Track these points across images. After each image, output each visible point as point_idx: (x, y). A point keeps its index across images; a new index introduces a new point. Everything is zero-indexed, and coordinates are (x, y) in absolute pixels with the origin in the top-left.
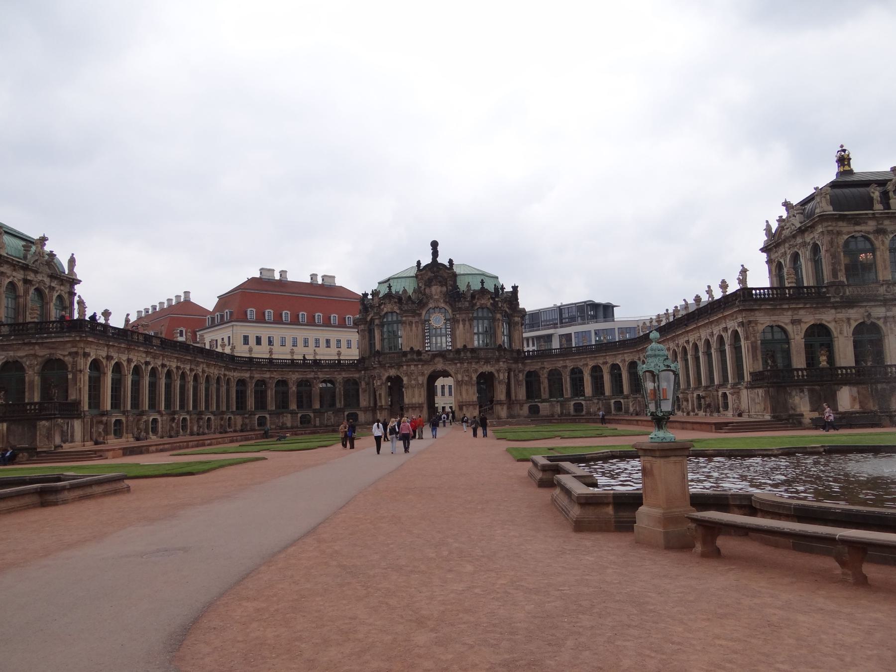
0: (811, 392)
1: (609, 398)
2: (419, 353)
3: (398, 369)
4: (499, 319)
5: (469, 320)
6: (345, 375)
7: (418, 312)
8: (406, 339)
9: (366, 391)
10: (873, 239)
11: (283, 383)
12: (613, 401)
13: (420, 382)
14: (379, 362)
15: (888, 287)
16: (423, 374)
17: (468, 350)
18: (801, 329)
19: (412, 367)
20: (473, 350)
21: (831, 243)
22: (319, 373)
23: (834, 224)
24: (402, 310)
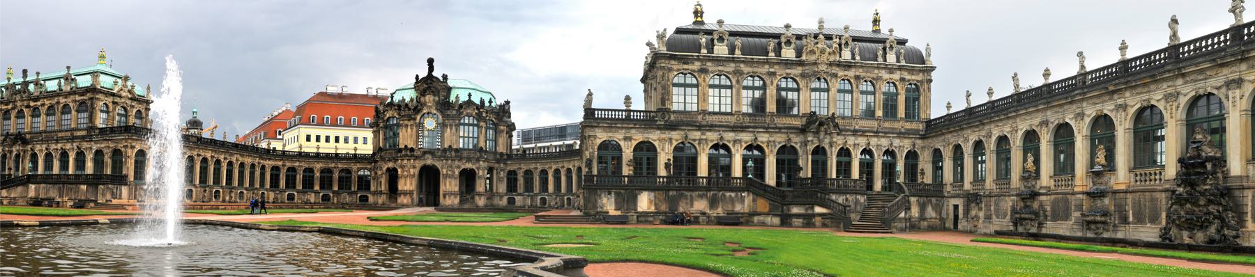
2: (412, 150)
4: (482, 127)
5: (456, 125)
6: (359, 166)
7: (413, 116)
8: (406, 138)
10: (697, 76)
12: (566, 197)
13: (412, 173)
14: (380, 156)
15: (704, 115)
16: (414, 167)
17: (453, 149)
18: (632, 145)
19: (406, 161)
20: (457, 150)
23: (667, 62)
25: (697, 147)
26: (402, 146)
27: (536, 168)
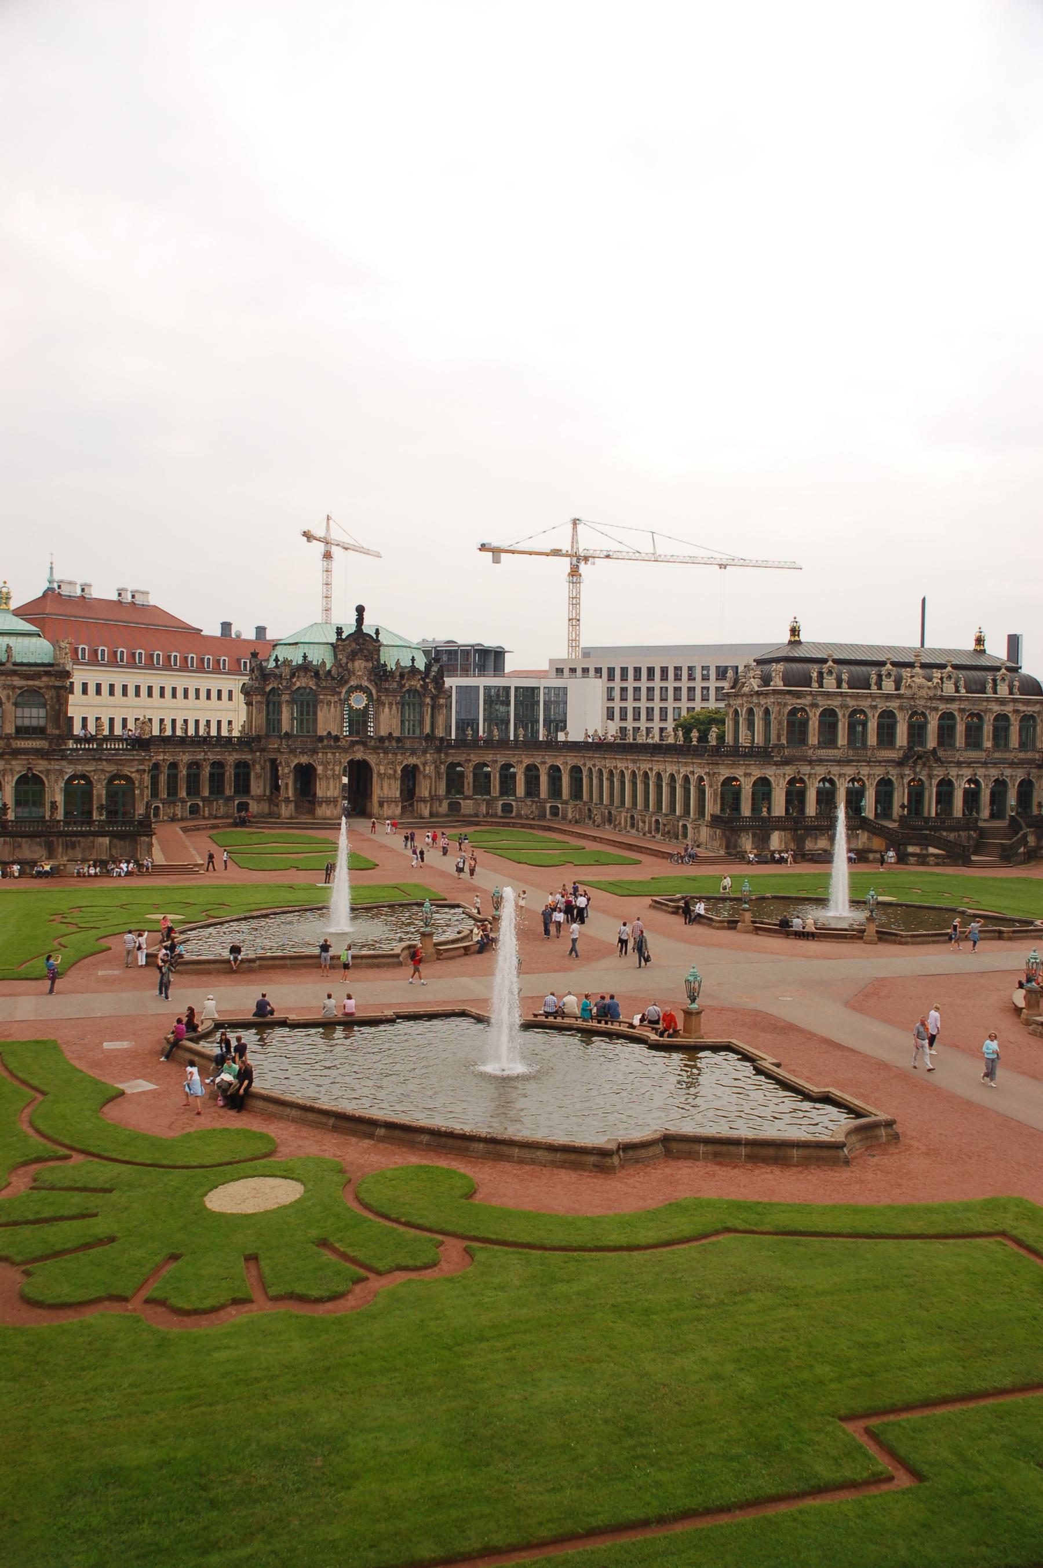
0: (754, 836)
1: (545, 802)
2: (337, 739)
3: (312, 756)
5: (396, 704)
9: (260, 777)
11: (174, 765)
12: (549, 805)
13: (337, 773)
14: (288, 746)
17: (393, 738)
19: (330, 755)
20: (399, 740)
21: (779, 712)
22: (209, 754)
24: (319, 686)
25: (807, 780)
26: (322, 732)
27: (496, 761)
